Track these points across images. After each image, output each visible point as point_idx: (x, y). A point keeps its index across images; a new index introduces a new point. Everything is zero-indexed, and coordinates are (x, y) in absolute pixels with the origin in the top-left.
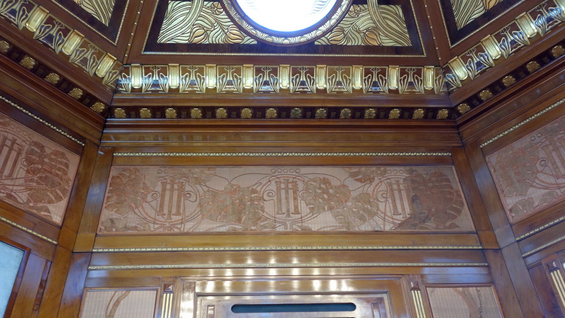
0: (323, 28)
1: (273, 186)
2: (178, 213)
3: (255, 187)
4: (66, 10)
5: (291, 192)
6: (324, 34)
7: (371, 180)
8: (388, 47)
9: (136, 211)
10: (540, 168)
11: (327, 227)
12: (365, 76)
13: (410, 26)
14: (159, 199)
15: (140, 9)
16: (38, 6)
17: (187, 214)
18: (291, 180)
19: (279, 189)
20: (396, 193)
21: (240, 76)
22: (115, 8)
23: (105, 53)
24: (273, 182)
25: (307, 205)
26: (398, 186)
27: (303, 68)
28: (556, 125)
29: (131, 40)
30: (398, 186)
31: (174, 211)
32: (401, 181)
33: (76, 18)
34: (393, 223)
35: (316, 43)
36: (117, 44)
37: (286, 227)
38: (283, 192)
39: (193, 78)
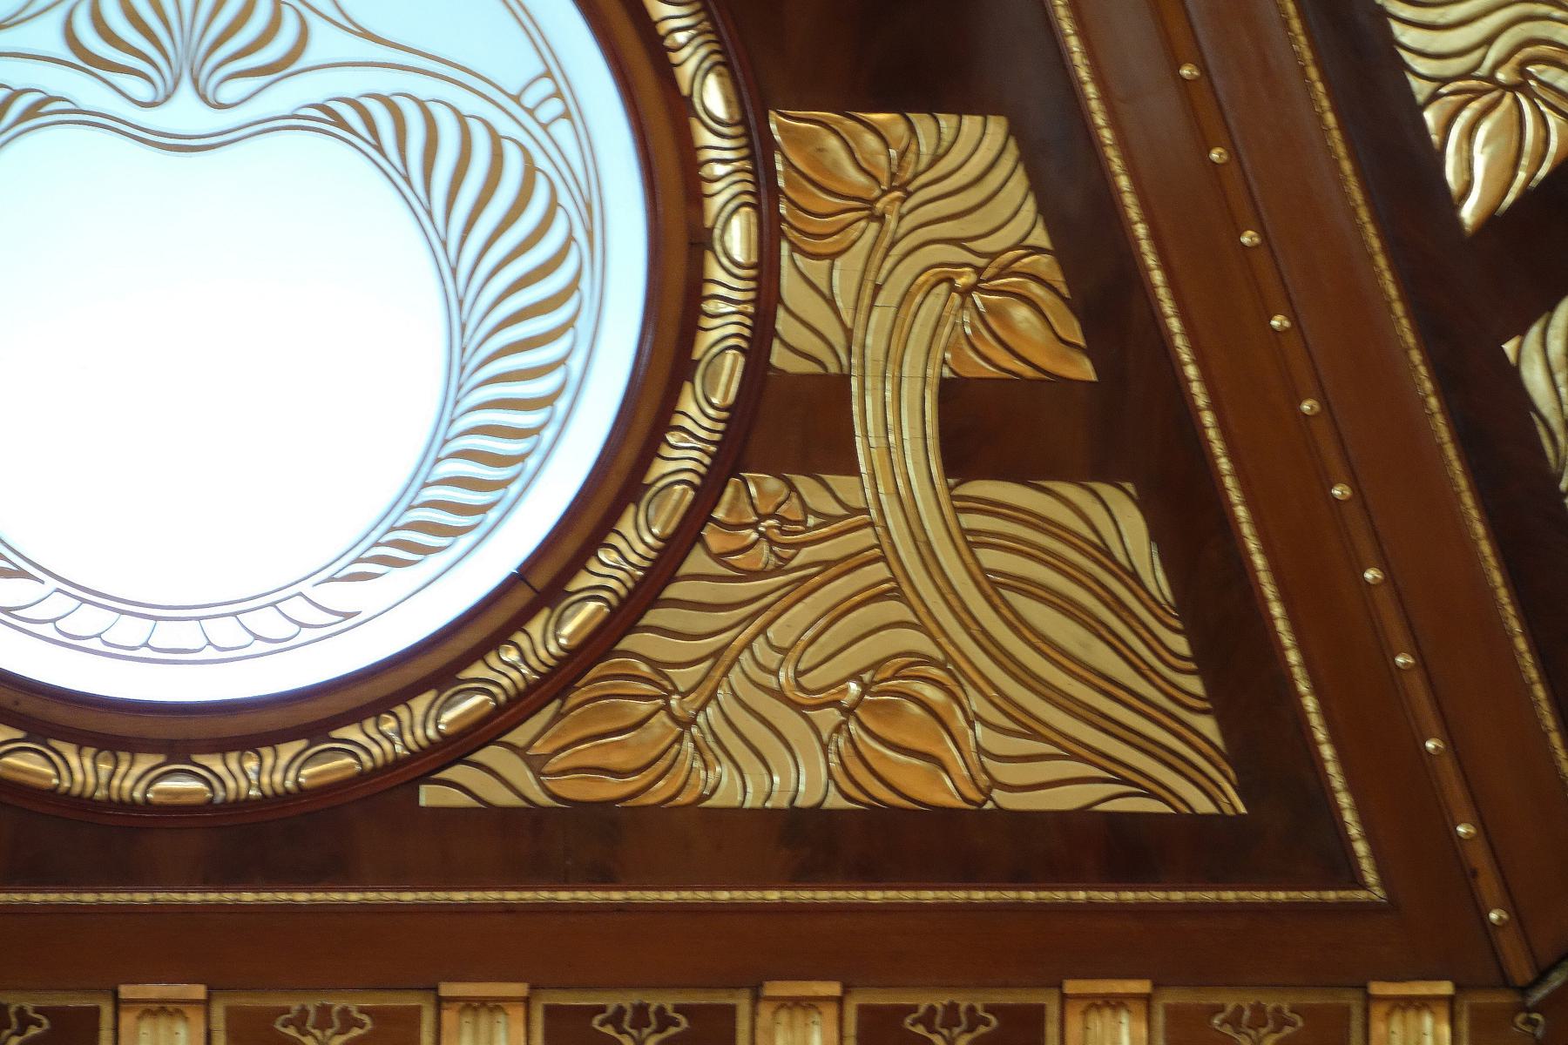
4: (928, 896)
15: (1365, 545)
16: (756, 999)
22: (1206, 660)
23: (1352, 1000)
29: (1455, 792)
33: (1020, 906)
36: (1384, 882)
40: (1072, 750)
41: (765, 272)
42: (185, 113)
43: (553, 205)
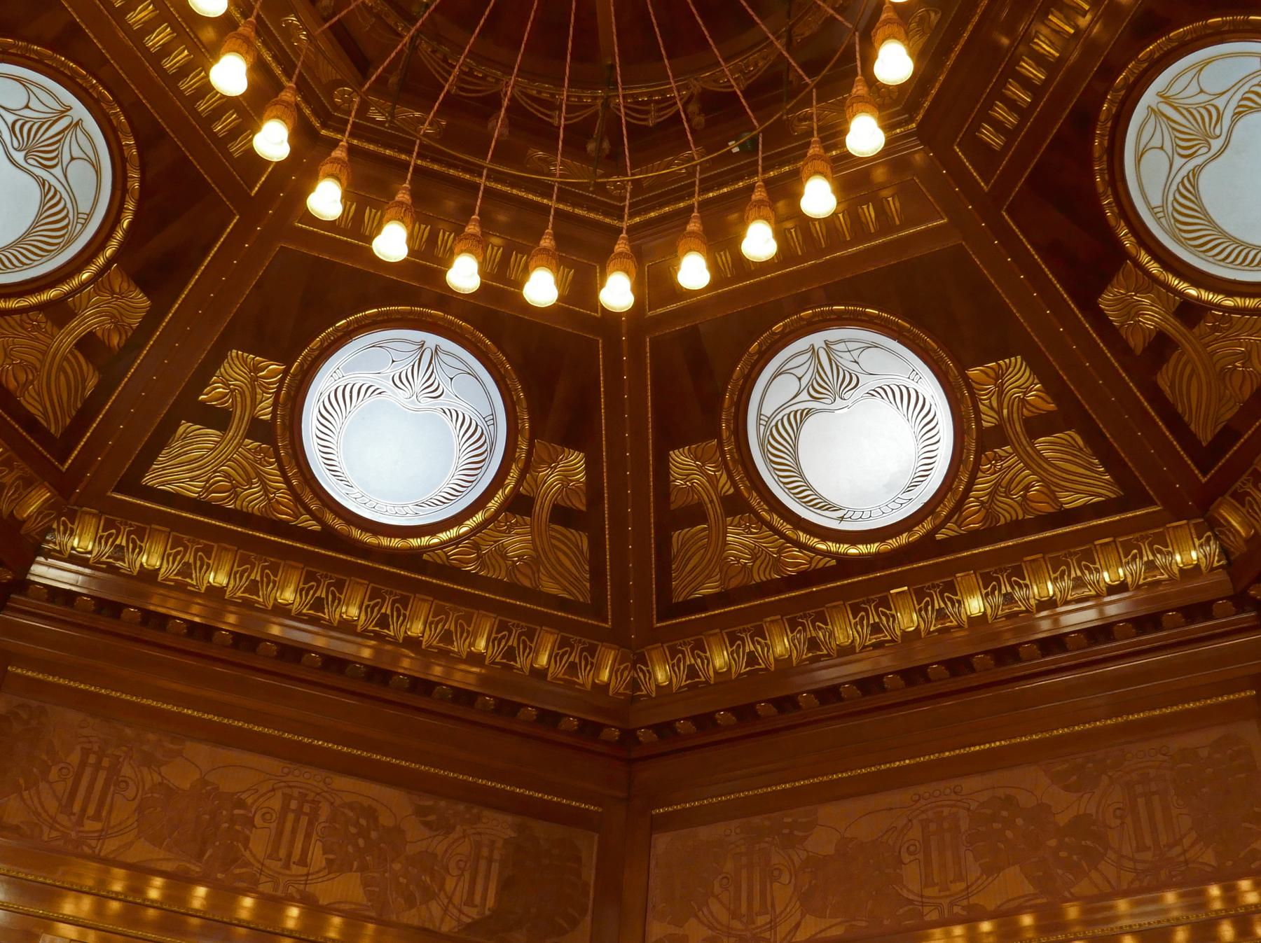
0: (444, 536)
1: (276, 803)
2: (97, 817)
3: (243, 796)
5: (304, 820)
6: (443, 544)
7: (450, 829)
8: (548, 594)
9: (26, 794)
10: (717, 889)
11: (346, 902)
12: (497, 633)
13: (597, 574)
14: (70, 782)
17: (112, 823)
18: (311, 796)
19: (285, 809)
20: (483, 864)
21: (276, 576)
24: (279, 794)
25: (325, 853)
26: (491, 851)
27: (391, 593)
28: (767, 823)
30: (491, 851)
31: (91, 811)
32: (499, 844)
34: (459, 920)
35: (425, 557)
37: (276, 889)
38: (291, 816)
39: (189, 558)
40: (44, 407)
41: (83, 285)
42: (19, 157)
43: (63, 236)
